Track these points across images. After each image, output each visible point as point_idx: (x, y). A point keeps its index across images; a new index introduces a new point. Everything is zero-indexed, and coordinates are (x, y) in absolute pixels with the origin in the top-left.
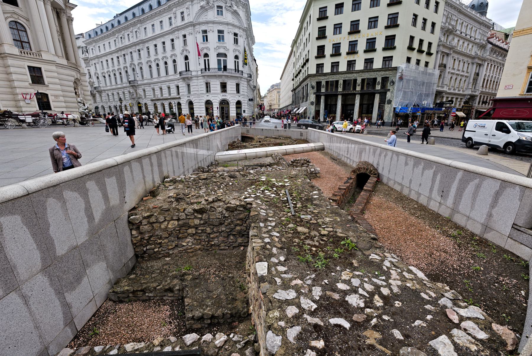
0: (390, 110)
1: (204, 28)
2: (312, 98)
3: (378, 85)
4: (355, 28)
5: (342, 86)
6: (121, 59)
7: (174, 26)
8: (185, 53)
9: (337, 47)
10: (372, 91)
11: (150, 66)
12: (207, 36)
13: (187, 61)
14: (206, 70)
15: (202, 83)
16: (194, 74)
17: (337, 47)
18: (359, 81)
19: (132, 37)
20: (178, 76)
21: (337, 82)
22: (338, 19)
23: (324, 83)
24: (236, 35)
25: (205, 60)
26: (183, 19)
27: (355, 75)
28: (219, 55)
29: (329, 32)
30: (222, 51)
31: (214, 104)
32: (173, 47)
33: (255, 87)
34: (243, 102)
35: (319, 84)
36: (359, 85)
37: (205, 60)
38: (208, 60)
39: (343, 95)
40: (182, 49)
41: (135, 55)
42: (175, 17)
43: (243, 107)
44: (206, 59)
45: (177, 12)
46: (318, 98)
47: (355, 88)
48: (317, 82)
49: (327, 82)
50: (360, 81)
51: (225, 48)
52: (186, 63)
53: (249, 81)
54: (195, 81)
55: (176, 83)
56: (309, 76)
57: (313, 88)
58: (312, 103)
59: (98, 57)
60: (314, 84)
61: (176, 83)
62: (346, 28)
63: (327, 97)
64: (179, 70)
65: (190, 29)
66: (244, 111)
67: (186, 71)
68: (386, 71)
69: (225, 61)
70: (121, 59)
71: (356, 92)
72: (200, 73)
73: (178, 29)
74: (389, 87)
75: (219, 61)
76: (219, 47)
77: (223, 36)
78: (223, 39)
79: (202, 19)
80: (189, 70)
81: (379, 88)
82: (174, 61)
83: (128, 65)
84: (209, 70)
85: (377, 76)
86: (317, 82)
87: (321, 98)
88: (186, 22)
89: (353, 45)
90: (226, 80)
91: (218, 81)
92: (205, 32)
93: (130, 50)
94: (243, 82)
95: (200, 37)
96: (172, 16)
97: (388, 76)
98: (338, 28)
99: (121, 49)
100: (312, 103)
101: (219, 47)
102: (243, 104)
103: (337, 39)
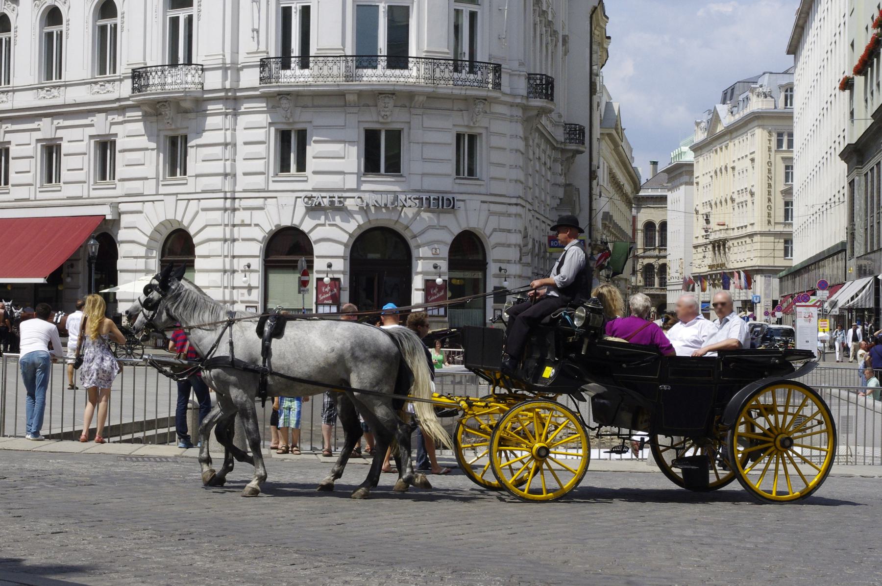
14: (286, 65)
15: (260, 135)
16: (214, 81)
20: (125, 89)
31: (317, 249)
33: (577, 133)
34: (490, 242)
43: (492, 268)
52: (175, 21)
53: (531, 120)
61: (100, 124)
72: (250, 78)
80: (189, 62)
90: (397, 119)
91: (353, 119)
94: (497, 126)
102: (493, 254)
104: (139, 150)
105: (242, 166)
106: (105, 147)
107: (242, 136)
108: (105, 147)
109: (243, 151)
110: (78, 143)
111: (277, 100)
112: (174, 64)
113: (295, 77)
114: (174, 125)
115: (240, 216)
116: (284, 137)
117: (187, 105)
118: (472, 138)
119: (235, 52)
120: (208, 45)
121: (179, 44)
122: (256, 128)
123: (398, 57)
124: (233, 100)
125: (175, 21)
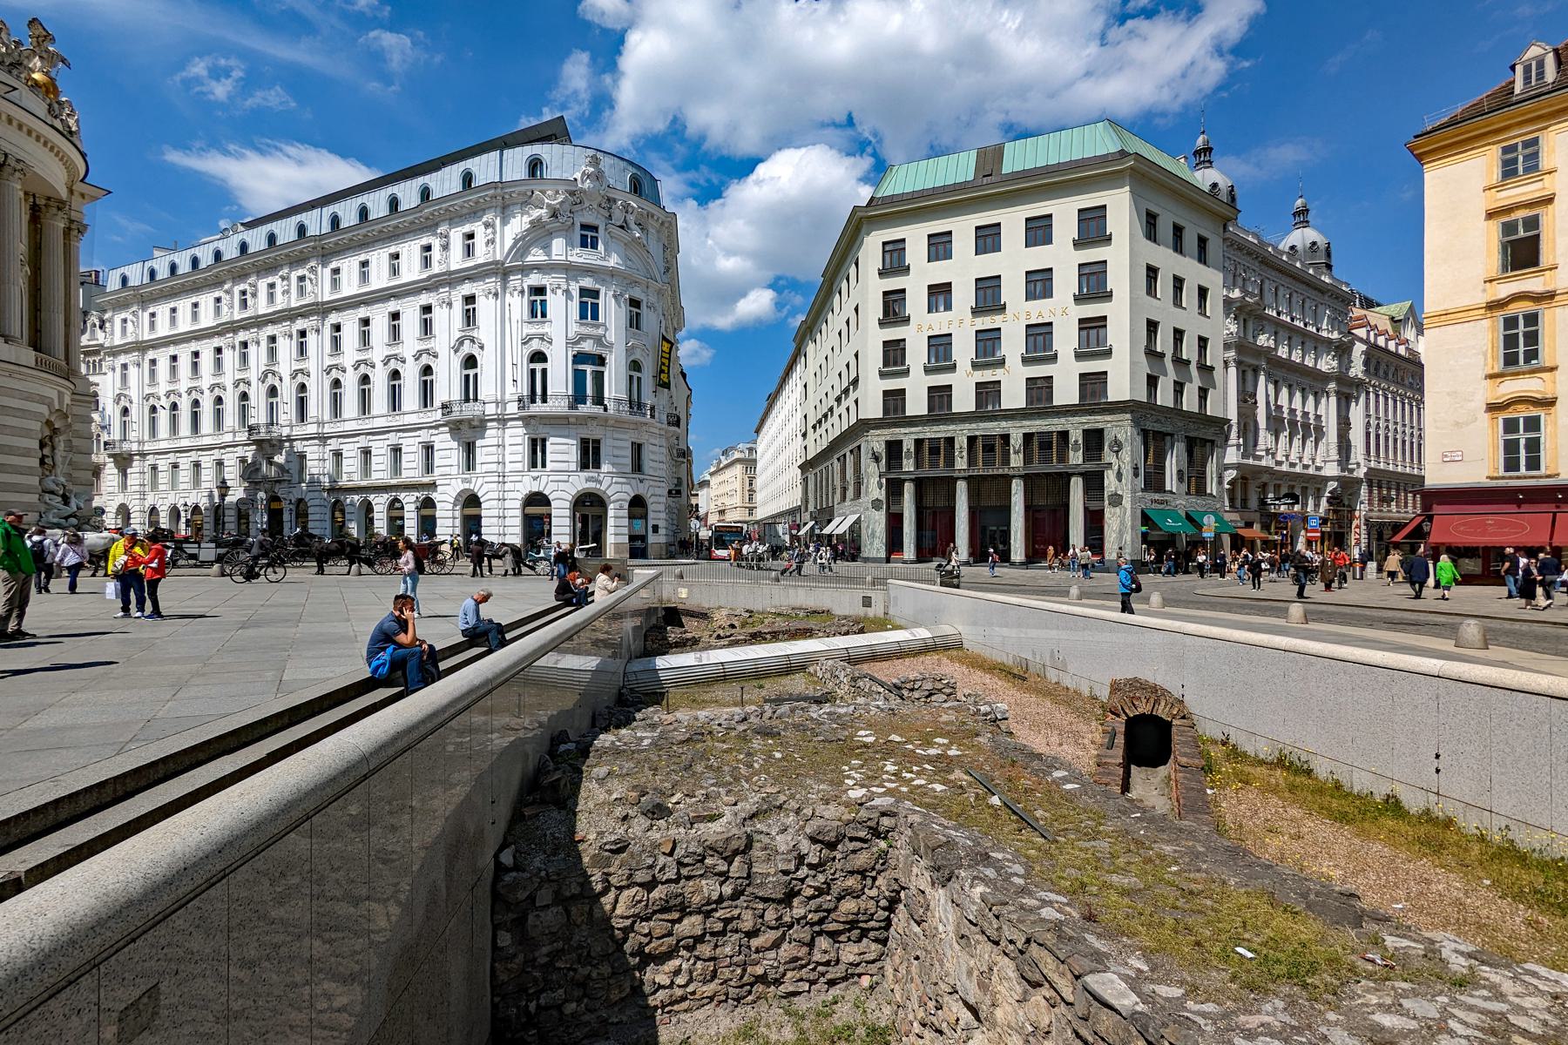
0: (1122, 523)
1: (535, 279)
2: (875, 489)
3: (1076, 450)
4: (988, 294)
5: (965, 454)
6: (230, 357)
7: (436, 268)
8: (467, 348)
9: (940, 345)
10: (1060, 468)
11: (337, 383)
12: (543, 302)
13: (471, 372)
14: (533, 401)
15: (519, 440)
17: (940, 345)
18: (1016, 441)
19: (286, 292)
21: (950, 441)
22: (940, 272)
23: (908, 445)
24: (635, 303)
25: (533, 372)
26: (469, 251)
27: (1004, 424)
28: (580, 358)
29: (916, 302)
30: (588, 347)
32: (427, 327)
34: (649, 501)
35: (894, 448)
36: (1016, 452)
37: (533, 372)
38: (544, 371)
39: (968, 479)
40: (458, 335)
41: (286, 348)
42: (445, 247)
43: (651, 515)
44: (538, 367)
45: (452, 233)
46: (894, 489)
47: (1006, 461)
48: (889, 444)
49: (919, 443)
50: (1020, 441)
51: (599, 340)
54: (494, 432)
55: (424, 436)
56: (864, 426)
57: (877, 459)
58: (876, 504)
59: (141, 347)
60: (880, 448)
61: (424, 436)
62: (964, 296)
63: (919, 483)
64: (440, 396)
65: (492, 283)
66: (656, 529)
67: (467, 400)
68: (1092, 412)
69: (599, 378)
70: (230, 357)
71: (1011, 473)
72: (512, 408)
73: (451, 279)
74: (1108, 456)
75: (579, 377)
76: (583, 338)
77: (595, 307)
78: (595, 316)
79: (536, 256)
80: (476, 399)
81: (1080, 461)
82: (427, 370)
83: (253, 375)
84: (544, 401)
85: (1068, 427)
86: (889, 444)
87: (901, 494)
88: (481, 261)
89: (988, 342)
92: (540, 291)
93: (270, 330)
95: (518, 305)
96: (436, 243)
97: (1100, 426)
98: (940, 294)
99: (234, 327)
100: (876, 504)
101: (583, 338)
102: (651, 508)
103: (940, 322)
104: (448, 452)
105: (507, 459)
106: (429, 449)
107: (508, 441)
108: (429, 449)
109: (508, 449)
110: (411, 447)
111: (527, 421)
112: (467, 400)
113: (538, 408)
114: (468, 433)
115: (508, 486)
116: (534, 442)
117: (476, 423)
118: (640, 446)
119: (503, 392)
120: (487, 390)
121: (470, 389)
122: (517, 437)
123: (599, 399)
124: (503, 421)
125: (467, 377)
